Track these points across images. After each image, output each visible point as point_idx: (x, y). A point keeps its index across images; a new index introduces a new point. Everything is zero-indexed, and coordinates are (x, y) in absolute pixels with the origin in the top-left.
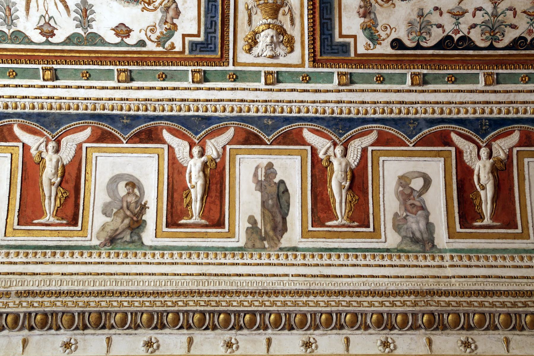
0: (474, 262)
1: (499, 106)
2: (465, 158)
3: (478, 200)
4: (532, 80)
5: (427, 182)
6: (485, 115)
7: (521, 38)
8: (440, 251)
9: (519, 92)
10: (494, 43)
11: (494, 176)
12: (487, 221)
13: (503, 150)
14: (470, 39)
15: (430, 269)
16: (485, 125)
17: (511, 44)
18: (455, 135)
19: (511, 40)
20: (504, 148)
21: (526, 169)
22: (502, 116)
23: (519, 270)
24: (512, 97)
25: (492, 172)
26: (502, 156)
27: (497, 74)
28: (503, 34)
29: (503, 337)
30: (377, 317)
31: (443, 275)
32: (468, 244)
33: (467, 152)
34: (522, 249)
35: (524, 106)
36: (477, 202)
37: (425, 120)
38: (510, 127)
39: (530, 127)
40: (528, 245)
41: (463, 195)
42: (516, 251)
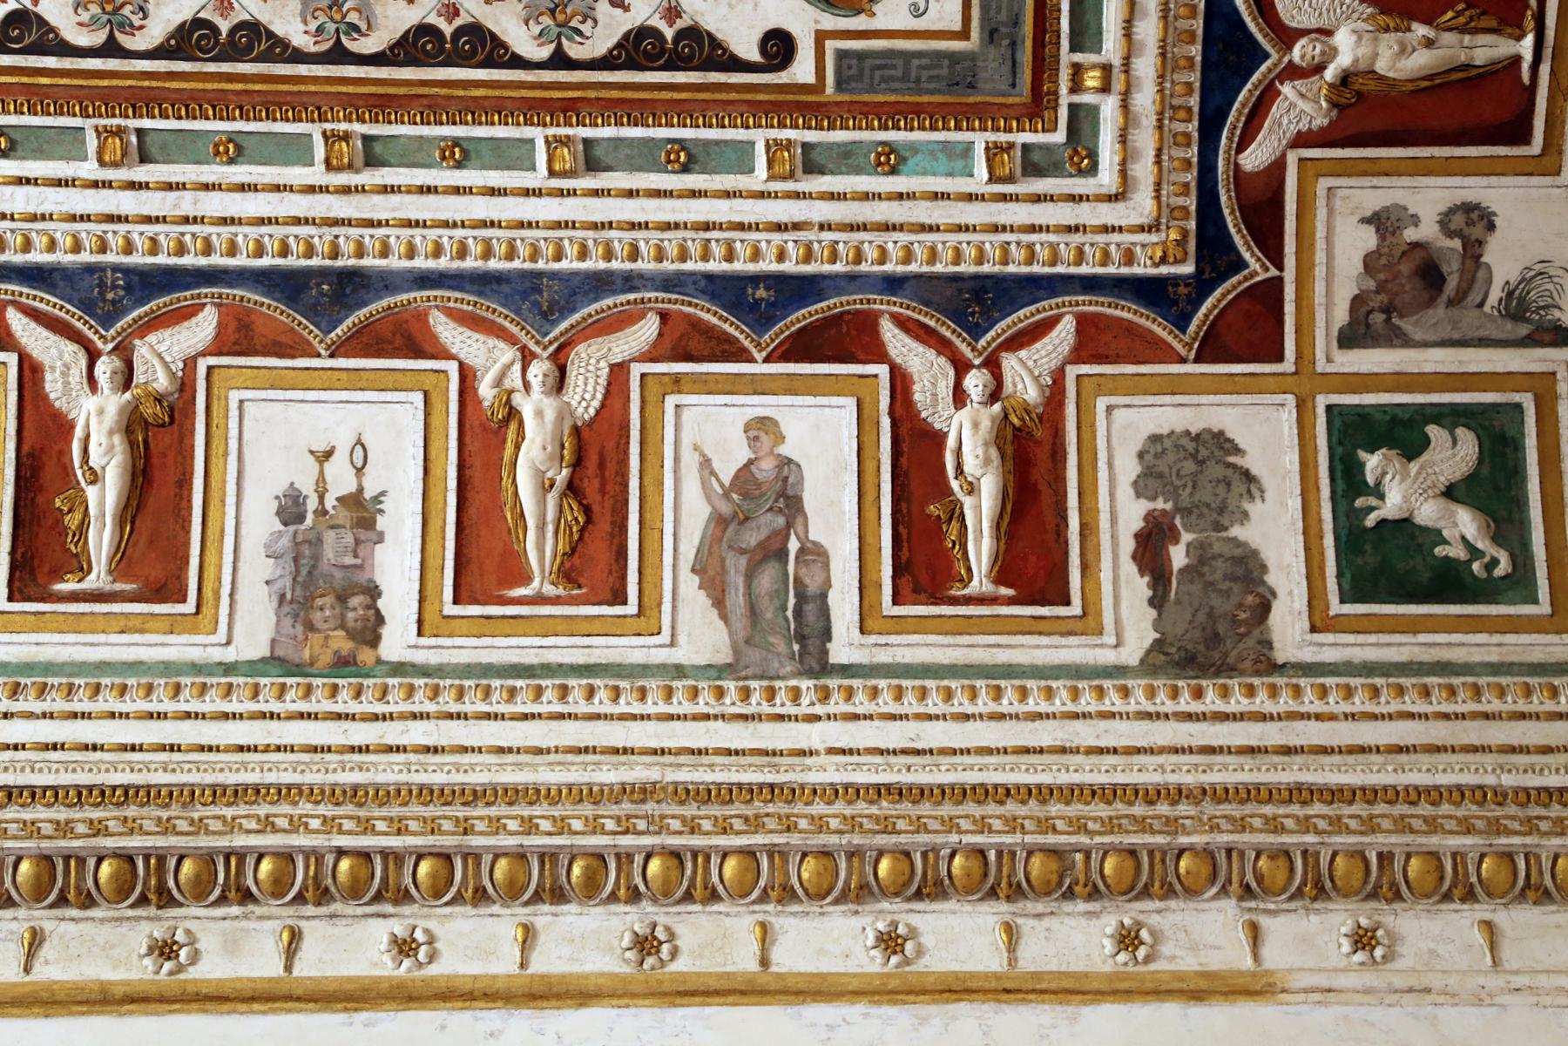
1: (150, 229)
2: (48, 387)
3: (78, 516)
4: (246, 152)
6: (110, 258)
7: (198, 23)
9: (206, 187)
10: (120, 37)
11: (132, 445)
12: (97, 578)
13: (166, 364)
14: (42, 21)
16: (114, 287)
17: (173, 42)
18: (19, 315)
19: (171, 28)
20: (168, 359)
22: (161, 259)
24: (186, 203)
26: (162, 383)
27: (140, 132)
28: (141, 9)
29: (26, 925)
30: (351, 867)
32: (25, 648)
33: (53, 368)
34: (186, 664)
35: (226, 231)
36: (72, 521)
38: (188, 294)
39: (249, 295)
40: (209, 649)
41: (32, 500)
42: (167, 668)
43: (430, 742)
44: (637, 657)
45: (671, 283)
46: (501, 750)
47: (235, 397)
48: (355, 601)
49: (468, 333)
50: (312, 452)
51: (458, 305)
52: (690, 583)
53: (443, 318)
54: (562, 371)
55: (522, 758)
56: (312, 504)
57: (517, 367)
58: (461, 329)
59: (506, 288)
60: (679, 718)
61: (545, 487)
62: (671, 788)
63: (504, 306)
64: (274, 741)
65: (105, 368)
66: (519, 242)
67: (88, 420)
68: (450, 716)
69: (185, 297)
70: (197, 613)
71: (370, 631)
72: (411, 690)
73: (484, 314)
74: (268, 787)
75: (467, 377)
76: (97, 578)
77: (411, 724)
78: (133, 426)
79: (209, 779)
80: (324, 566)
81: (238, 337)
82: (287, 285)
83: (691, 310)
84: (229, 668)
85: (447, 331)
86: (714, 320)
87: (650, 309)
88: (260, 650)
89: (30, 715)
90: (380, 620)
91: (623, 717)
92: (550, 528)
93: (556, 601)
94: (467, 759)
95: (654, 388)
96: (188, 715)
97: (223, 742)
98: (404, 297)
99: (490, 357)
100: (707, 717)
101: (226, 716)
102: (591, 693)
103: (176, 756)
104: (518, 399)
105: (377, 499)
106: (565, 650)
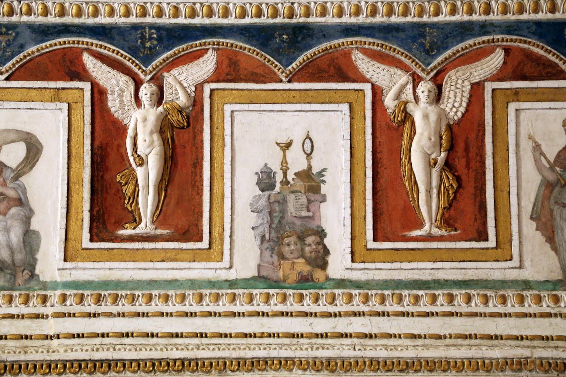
0: (35, 307)
2: (110, 104)
3: (131, 187)
5: (34, 151)
6: (148, 20)
8: (45, 286)
11: (164, 140)
13: (184, 88)
15: (15, 321)
16: (151, 39)
18: (91, 58)
20: (185, 85)
21: (227, 126)
22: (181, 20)
23: (189, 320)
25: (161, 132)
26: (182, 100)
31: (38, 332)
32: (102, 272)
33: (113, 92)
34: (205, 281)
36: (128, 190)
37: (31, 27)
38: (198, 42)
39: (236, 43)
40: (218, 272)
41: (102, 177)
42: (193, 284)
43: (366, 331)
44: (497, 275)
45: (512, 28)
46: (414, 336)
47: (228, 108)
48: (310, 240)
49: (377, 65)
50: (278, 144)
51: (371, 47)
52: (530, 227)
53: (361, 55)
54: (440, 88)
55: (428, 341)
56: (279, 177)
57: (410, 87)
58: (372, 63)
59: (402, 35)
60: (530, 315)
61: (431, 164)
62: (538, 362)
63: (400, 46)
64: (266, 330)
65: (146, 91)
66: (411, 4)
67: (136, 125)
68: (378, 314)
69: (196, 44)
70: (210, 248)
71: (321, 259)
72: (350, 298)
73: (388, 52)
74: (273, 359)
75: (377, 93)
76: (145, 226)
77: (353, 319)
78: (165, 128)
79: (235, 354)
80: (289, 217)
81: (230, 70)
82: (260, 35)
83: (526, 46)
84: (232, 284)
85: (363, 63)
86: (542, 52)
87: (498, 46)
88: (250, 271)
89: (110, 315)
90: (326, 252)
91: (492, 315)
92: (435, 191)
93: (441, 239)
94: (391, 342)
95: (500, 98)
96: (210, 314)
97: (233, 332)
98: (336, 42)
99: (392, 81)
100: (549, 315)
101: (233, 314)
102: (469, 299)
103: (205, 341)
104: (411, 107)
105: (321, 173)
106: (448, 271)
